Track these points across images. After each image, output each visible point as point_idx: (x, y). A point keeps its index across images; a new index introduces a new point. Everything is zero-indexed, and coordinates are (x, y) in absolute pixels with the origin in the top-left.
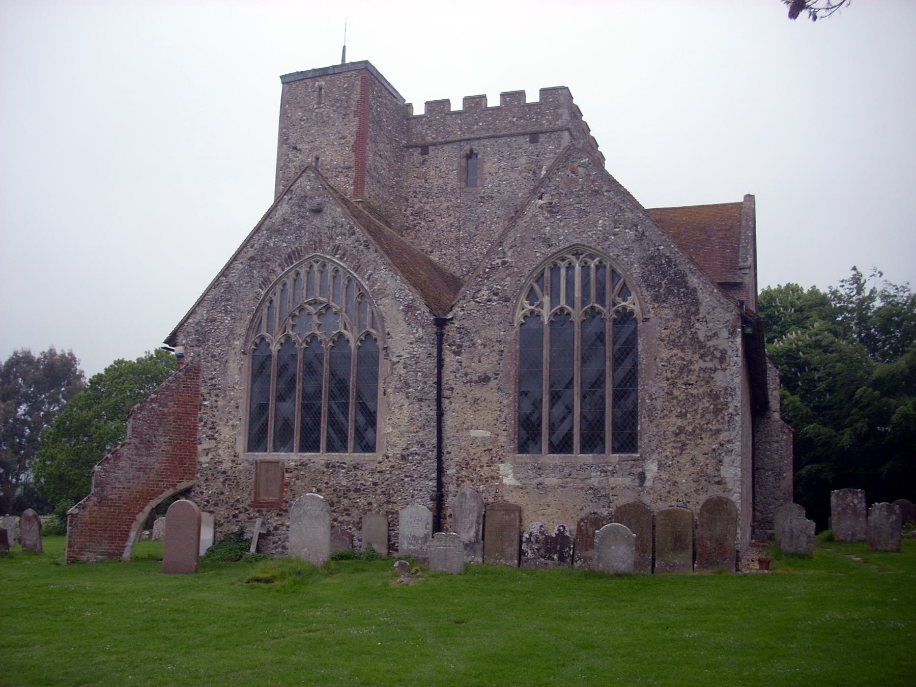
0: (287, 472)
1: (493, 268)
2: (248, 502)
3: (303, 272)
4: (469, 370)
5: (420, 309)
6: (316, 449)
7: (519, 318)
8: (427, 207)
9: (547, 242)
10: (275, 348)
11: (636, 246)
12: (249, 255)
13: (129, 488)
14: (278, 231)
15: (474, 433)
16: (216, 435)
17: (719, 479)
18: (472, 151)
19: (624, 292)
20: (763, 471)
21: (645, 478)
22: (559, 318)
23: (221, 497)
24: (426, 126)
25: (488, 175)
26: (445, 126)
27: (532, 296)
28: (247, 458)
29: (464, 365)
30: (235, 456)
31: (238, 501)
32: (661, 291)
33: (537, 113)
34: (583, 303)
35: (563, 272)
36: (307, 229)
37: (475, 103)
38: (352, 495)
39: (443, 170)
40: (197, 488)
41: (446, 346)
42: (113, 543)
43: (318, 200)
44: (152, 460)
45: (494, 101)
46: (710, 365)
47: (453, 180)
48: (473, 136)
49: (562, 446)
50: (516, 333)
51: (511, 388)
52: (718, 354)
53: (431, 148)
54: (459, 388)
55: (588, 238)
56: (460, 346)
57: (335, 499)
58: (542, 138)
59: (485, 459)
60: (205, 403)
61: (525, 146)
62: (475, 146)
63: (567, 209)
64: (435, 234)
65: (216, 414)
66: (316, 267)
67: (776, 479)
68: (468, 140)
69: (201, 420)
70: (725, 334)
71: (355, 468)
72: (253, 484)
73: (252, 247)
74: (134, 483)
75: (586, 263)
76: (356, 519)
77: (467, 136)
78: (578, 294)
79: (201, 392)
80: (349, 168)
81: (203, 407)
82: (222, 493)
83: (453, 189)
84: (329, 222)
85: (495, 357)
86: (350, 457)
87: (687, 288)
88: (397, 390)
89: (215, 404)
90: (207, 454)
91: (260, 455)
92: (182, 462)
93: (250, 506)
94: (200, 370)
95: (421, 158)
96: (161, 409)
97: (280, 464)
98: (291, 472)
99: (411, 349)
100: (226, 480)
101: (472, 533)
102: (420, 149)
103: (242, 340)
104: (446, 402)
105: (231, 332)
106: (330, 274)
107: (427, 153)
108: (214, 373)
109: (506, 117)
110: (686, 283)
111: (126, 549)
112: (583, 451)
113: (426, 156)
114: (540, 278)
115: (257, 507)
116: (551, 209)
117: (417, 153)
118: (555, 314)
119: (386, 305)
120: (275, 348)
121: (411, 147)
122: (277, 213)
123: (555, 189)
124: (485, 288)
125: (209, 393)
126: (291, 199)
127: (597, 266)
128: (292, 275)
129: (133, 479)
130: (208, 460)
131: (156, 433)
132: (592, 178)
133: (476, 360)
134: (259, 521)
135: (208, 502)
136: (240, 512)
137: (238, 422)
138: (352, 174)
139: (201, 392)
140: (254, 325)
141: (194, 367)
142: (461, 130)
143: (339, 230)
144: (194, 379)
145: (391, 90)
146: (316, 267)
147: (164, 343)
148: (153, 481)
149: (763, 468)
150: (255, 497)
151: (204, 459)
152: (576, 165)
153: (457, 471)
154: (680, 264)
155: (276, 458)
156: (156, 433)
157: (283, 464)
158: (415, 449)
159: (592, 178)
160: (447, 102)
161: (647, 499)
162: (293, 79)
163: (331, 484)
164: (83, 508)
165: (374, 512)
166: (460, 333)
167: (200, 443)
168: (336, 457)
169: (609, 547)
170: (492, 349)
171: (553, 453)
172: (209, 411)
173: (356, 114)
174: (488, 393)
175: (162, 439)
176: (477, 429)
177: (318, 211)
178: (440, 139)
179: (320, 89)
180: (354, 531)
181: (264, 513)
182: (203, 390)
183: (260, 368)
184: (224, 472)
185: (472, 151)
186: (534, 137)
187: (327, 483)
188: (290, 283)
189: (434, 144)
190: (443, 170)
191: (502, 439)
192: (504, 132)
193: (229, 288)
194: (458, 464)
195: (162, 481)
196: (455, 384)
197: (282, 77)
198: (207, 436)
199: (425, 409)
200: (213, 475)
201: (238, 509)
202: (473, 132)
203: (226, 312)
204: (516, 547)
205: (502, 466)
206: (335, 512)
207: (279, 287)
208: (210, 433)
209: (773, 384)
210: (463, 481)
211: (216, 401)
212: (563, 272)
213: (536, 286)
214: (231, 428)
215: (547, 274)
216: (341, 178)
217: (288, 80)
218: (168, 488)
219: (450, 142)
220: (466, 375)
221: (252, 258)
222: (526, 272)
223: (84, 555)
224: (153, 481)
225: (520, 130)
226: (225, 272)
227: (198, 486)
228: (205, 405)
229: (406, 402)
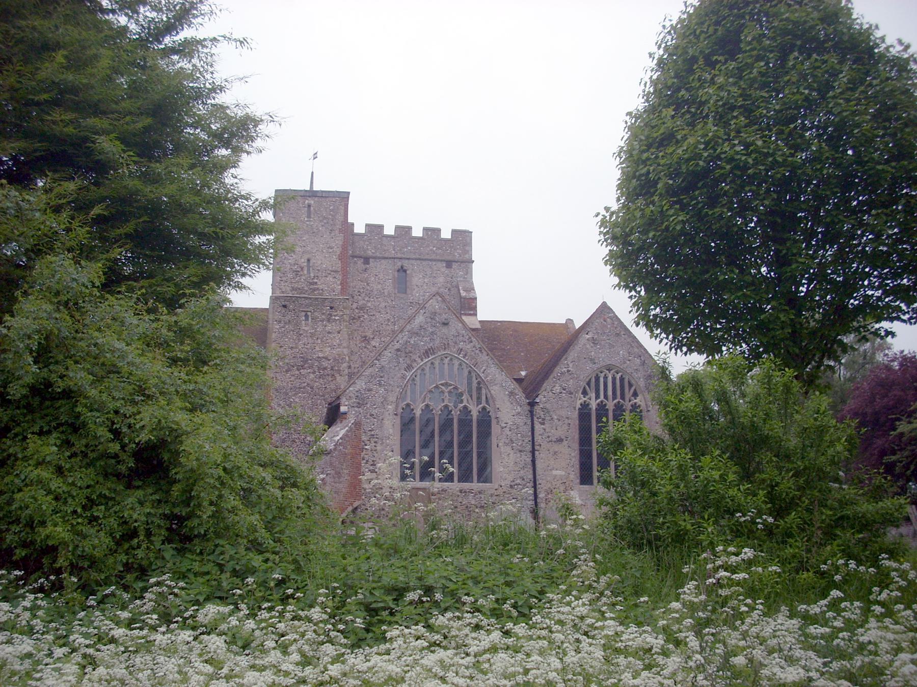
1: (562, 373)
3: (437, 363)
7: (578, 406)
8: (369, 304)
9: (592, 361)
10: (418, 412)
11: (641, 368)
12: (396, 347)
14: (417, 334)
15: (554, 472)
18: (402, 267)
19: (635, 395)
22: (602, 409)
23: (383, 512)
26: (382, 245)
27: (585, 393)
33: (451, 247)
34: (614, 398)
35: (602, 380)
37: (403, 231)
41: (535, 419)
43: (444, 316)
44: (341, 486)
45: (417, 232)
47: (389, 286)
51: (576, 446)
54: (545, 445)
55: (615, 361)
56: (544, 419)
58: (455, 266)
59: (562, 488)
61: (443, 270)
62: (406, 264)
63: (603, 343)
65: (376, 455)
66: (446, 361)
71: (480, 493)
77: (399, 255)
78: (610, 393)
80: (336, 271)
83: (389, 294)
84: (453, 332)
85: (565, 427)
86: (475, 485)
88: (506, 444)
89: (374, 448)
91: (411, 484)
92: (355, 488)
95: (364, 267)
103: (394, 405)
104: (537, 453)
105: (385, 399)
106: (456, 367)
109: (428, 246)
114: (589, 384)
116: (594, 341)
117: (360, 262)
118: (598, 405)
119: (495, 390)
120: (418, 412)
121: (356, 257)
128: (429, 365)
138: (339, 277)
140: (402, 396)
143: (461, 338)
146: (446, 361)
151: (366, 486)
158: (518, 481)
160: (381, 227)
168: (466, 486)
172: (370, 453)
173: (340, 231)
174: (563, 448)
177: (445, 324)
178: (378, 254)
179: (309, 206)
182: (364, 438)
183: (407, 424)
188: (427, 369)
189: (375, 258)
191: (572, 477)
192: (427, 257)
194: (546, 491)
199: (524, 457)
202: (404, 253)
203: (380, 385)
205: (572, 493)
207: (419, 371)
208: (371, 468)
212: (602, 380)
215: (593, 380)
216: (330, 278)
221: (398, 350)
222: (582, 377)
225: (438, 257)
229: (512, 452)
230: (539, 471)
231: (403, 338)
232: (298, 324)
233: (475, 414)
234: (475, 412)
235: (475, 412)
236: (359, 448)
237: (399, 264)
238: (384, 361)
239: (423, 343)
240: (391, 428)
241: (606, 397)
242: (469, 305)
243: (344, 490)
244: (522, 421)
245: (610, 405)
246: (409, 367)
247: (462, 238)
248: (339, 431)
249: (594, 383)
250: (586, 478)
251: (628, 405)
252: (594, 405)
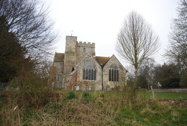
6: (90, 80)
10: (86, 70)
19: (118, 68)
22: (113, 70)
27: (110, 68)
28: (83, 80)
45: (87, 43)
47: (82, 51)
55: (115, 63)
86: (94, 81)
91: (84, 80)
119: (97, 67)
120: (86, 70)
174: (107, 76)
183: (84, 71)
186: (91, 48)
217: (67, 36)
230: (103, 80)
231: (84, 59)
232: (69, 56)
233: (94, 70)
234: (94, 70)
235: (94, 70)
236: (77, 75)
238: (81, 62)
239: (87, 60)
240: (81, 72)
242: (94, 54)
244: (101, 71)
245: (114, 70)
246: (85, 63)
247: (94, 44)
248: (74, 72)
249: (112, 66)
250: (110, 80)
251: (116, 70)
252: (111, 69)
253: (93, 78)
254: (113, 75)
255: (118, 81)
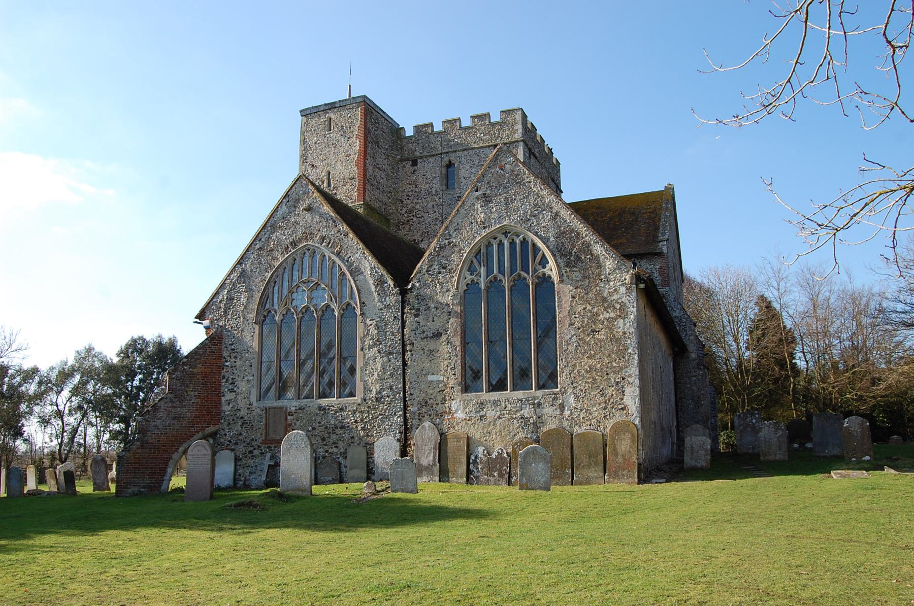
0: (289, 415)
2: (260, 440)
4: (425, 328)
5: (387, 283)
8: (418, 207)
12: (258, 246)
13: (166, 434)
16: (235, 389)
17: (623, 406)
18: (450, 162)
20: (685, 400)
21: (564, 407)
22: (494, 285)
23: (240, 437)
24: (415, 144)
25: (463, 179)
27: (471, 270)
29: (421, 324)
30: (250, 405)
31: (252, 440)
32: (572, 258)
34: (512, 270)
35: (495, 247)
36: (301, 224)
38: (339, 431)
39: (428, 177)
40: (222, 431)
42: (153, 478)
46: (612, 315)
47: (437, 185)
48: (450, 150)
49: (500, 386)
50: (460, 297)
51: (457, 341)
52: (618, 306)
53: (419, 160)
54: (419, 344)
57: (326, 435)
60: (227, 364)
62: (452, 157)
64: (424, 227)
67: (695, 406)
68: (447, 153)
69: (224, 377)
70: (623, 290)
71: (341, 409)
72: (264, 426)
73: (260, 241)
74: (170, 429)
75: (513, 240)
76: (342, 450)
77: (446, 150)
78: (507, 264)
79: (224, 355)
81: (225, 367)
82: (241, 434)
83: (436, 192)
87: (592, 255)
90: (229, 403)
93: (261, 443)
94: (222, 338)
96: (191, 370)
97: (284, 409)
98: (292, 415)
99: (381, 315)
100: (244, 423)
101: (431, 458)
102: (411, 162)
107: (416, 165)
108: (233, 340)
110: (591, 251)
111: (164, 482)
112: (514, 389)
113: (416, 167)
115: (267, 444)
121: (404, 160)
122: (278, 213)
123: (488, 183)
124: (436, 263)
125: (230, 356)
126: (288, 201)
127: (521, 242)
129: (169, 426)
130: (229, 409)
131: (188, 389)
132: (516, 173)
133: (431, 319)
134: (268, 455)
135: (230, 441)
136: (255, 449)
137: (251, 378)
139: (224, 355)
140: (262, 303)
141: (218, 336)
142: (441, 146)
144: (217, 345)
145: (386, 117)
147: (196, 318)
148: (186, 427)
149: (685, 398)
150: (266, 436)
151: (226, 408)
152: (503, 163)
153: (418, 408)
154: (586, 236)
155: (281, 404)
156: (188, 389)
157: (286, 408)
159: (516, 173)
161: (565, 424)
162: (309, 112)
163: (323, 423)
164: (129, 451)
165: (356, 444)
166: (418, 299)
167: (223, 396)
169: (531, 465)
170: (443, 311)
171: (492, 391)
175: (192, 393)
176: (433, 374)
178: (425, 154)
180: (341, 460)
181: (273, 448)
182: (225, 354)
184: (242, 418)
185: (450, 162)
187: (319, 423)
189: (421, 158)
190: (428, 177)
193: (243, 274)
194: (419, 403)
195: (193, 427)
196: (415, 340)
197: (301, 111)
198: (229, 390)
200: (233, 420)
201: (252, 446)
204: (465, 467)
206: (326, 445)
209: (690, 330)
210: (423, 417)
211: (235, 362)
212: (495, 247)
213: (475, 260)
214: (246, 382)
215: (483, 250)
218: (198, 432)
219: (433, 156)
220: (424, 332)
223: (129, 488)
224: (186, 427)
226: (240, 262)
227: (223, 429)
228: (227, 366)
237: (446, 159)
241: (502, 271)
243: (189, 415)
249: (481, 255)
253: (331, 384)
254: (519, 323)
255: (549, 380)
